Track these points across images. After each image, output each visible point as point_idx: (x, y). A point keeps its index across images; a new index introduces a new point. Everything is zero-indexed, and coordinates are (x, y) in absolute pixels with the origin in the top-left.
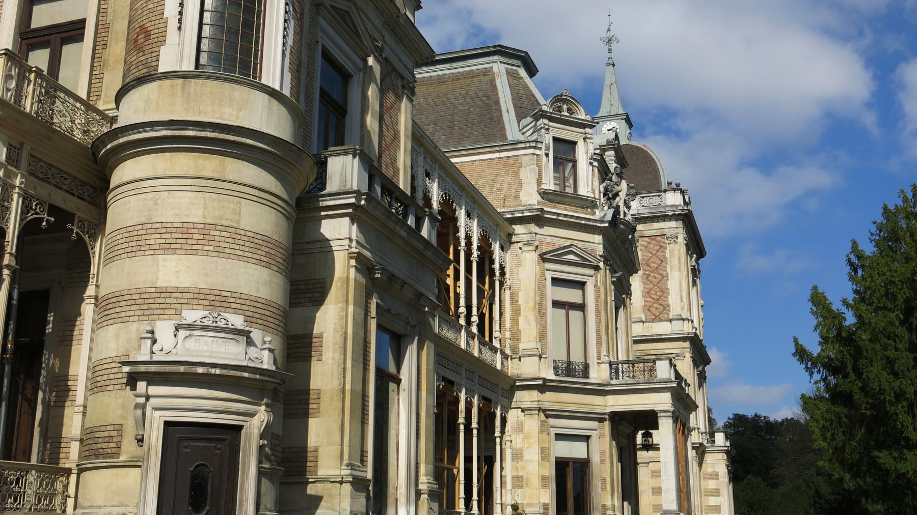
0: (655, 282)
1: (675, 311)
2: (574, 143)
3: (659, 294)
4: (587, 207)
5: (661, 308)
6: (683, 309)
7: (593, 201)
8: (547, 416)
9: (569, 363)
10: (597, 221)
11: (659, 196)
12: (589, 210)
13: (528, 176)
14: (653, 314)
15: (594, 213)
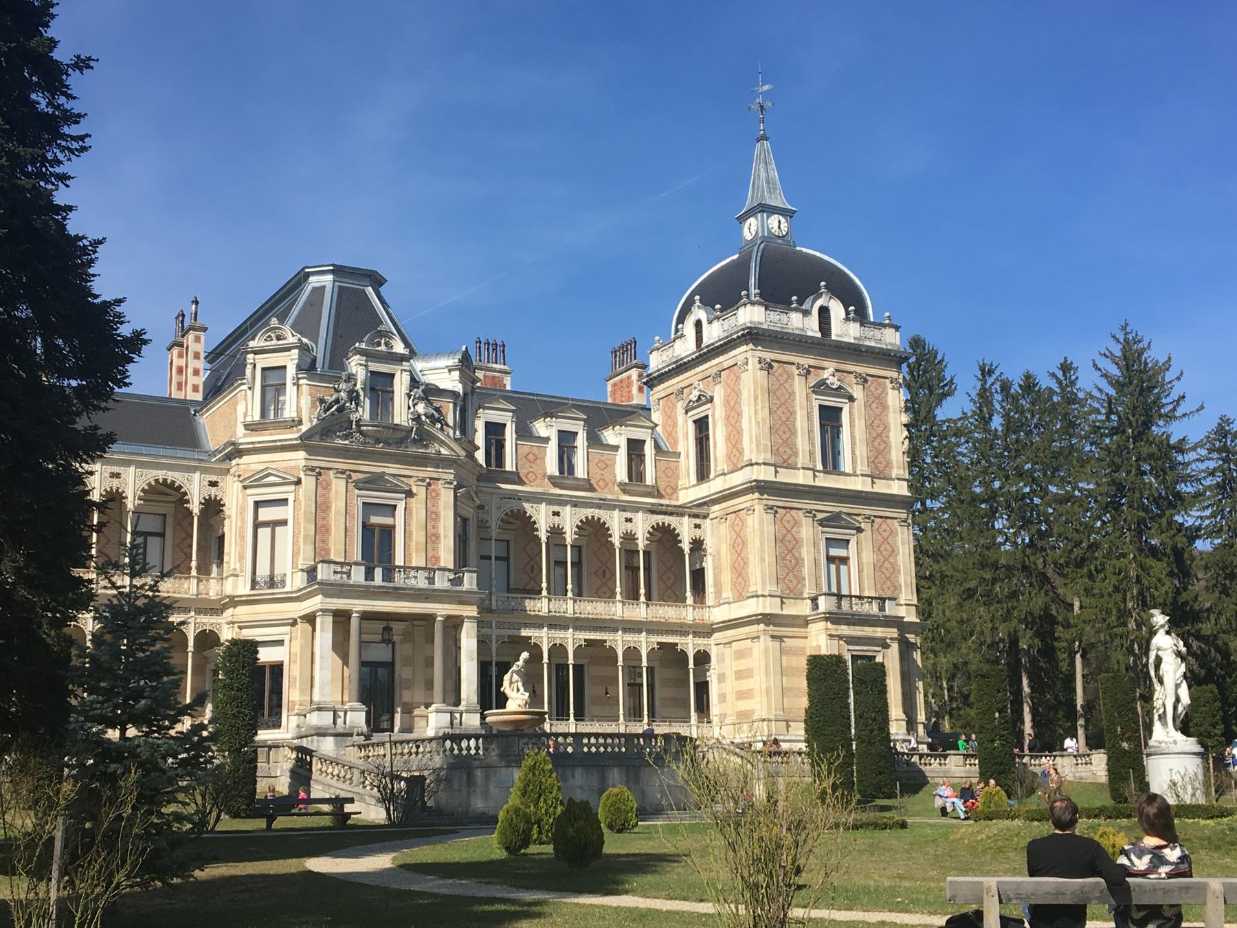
0: (733, 422)
1: (750, 453)
2: (284, 367)
3: (736, 437)
4: (292, 427)
5: (737, 453)
6: (751, 451)
7: (293, 421)
8: (240, 628)
9: (272, 577)
10: (291, 440)
11: (735, 314)
12: (295, 429)
13: (241, 409)
14: (733, 462)
15: (301, 430)
